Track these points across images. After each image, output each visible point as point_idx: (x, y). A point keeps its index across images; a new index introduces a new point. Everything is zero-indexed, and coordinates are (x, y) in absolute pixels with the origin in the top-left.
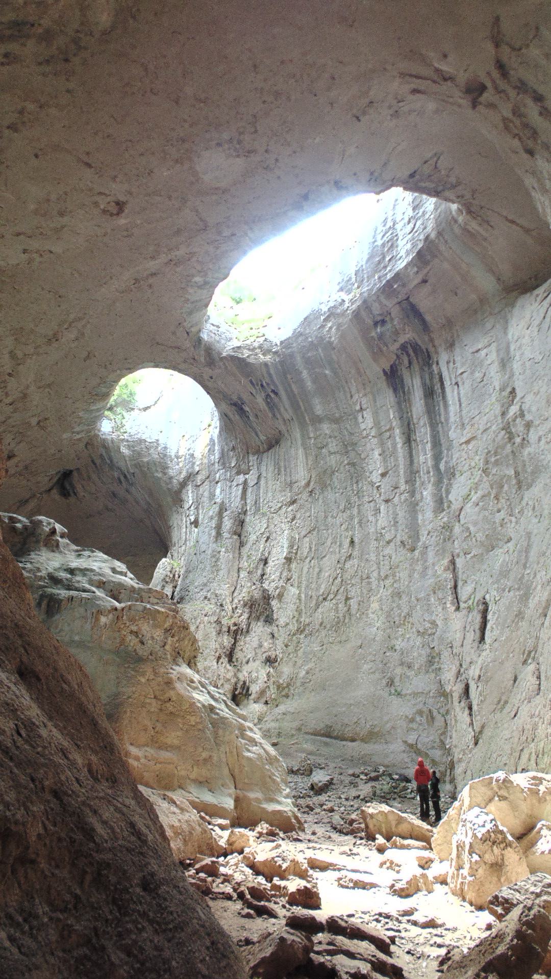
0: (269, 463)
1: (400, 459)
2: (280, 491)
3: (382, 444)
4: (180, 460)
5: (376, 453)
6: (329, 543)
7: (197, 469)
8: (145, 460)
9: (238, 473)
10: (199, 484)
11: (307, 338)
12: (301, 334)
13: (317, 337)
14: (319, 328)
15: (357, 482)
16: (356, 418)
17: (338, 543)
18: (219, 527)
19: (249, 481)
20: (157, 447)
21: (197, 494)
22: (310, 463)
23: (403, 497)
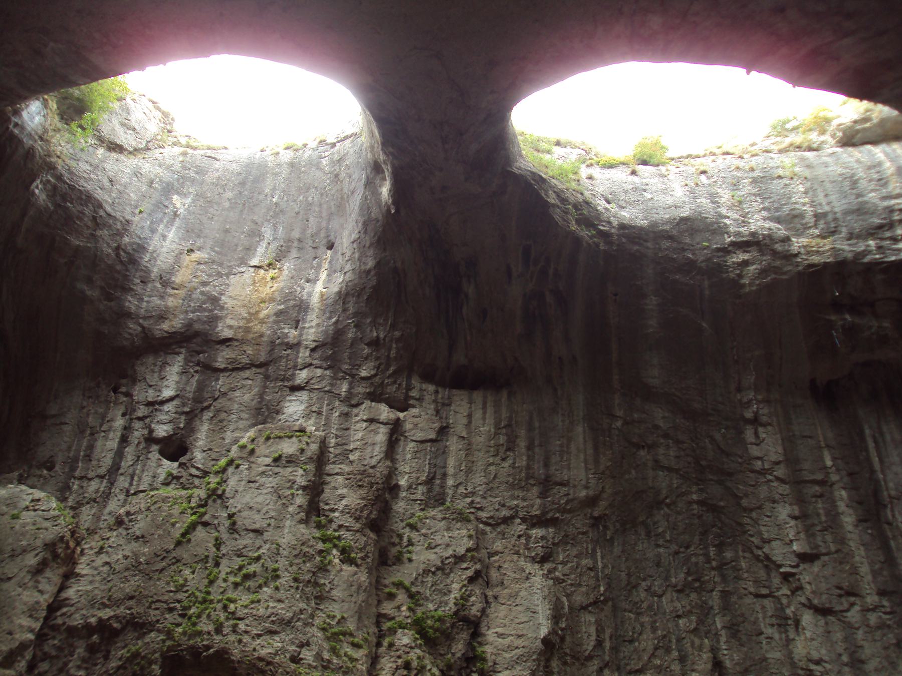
0: (478, 415)
1: (851, 543)
2: (512, 486)
3: (800, 500)
4: (169, 291)
5: (784, 512)
6: (647, 642)
7: (227, 333)
8: (76, 242)
9: (375, 397)
10: (220, 363)
11: (684, 250)
12: (671, 238)
13: (708, 260)
14: (718, 250)
15: (720, 547)
16: (740, 432)
17: (675, 654)
18: (315, 489)
19: (408, 426)
20: (119, 234)
21: (201, 387)
22: (605, 462)
23: (873, 618)
